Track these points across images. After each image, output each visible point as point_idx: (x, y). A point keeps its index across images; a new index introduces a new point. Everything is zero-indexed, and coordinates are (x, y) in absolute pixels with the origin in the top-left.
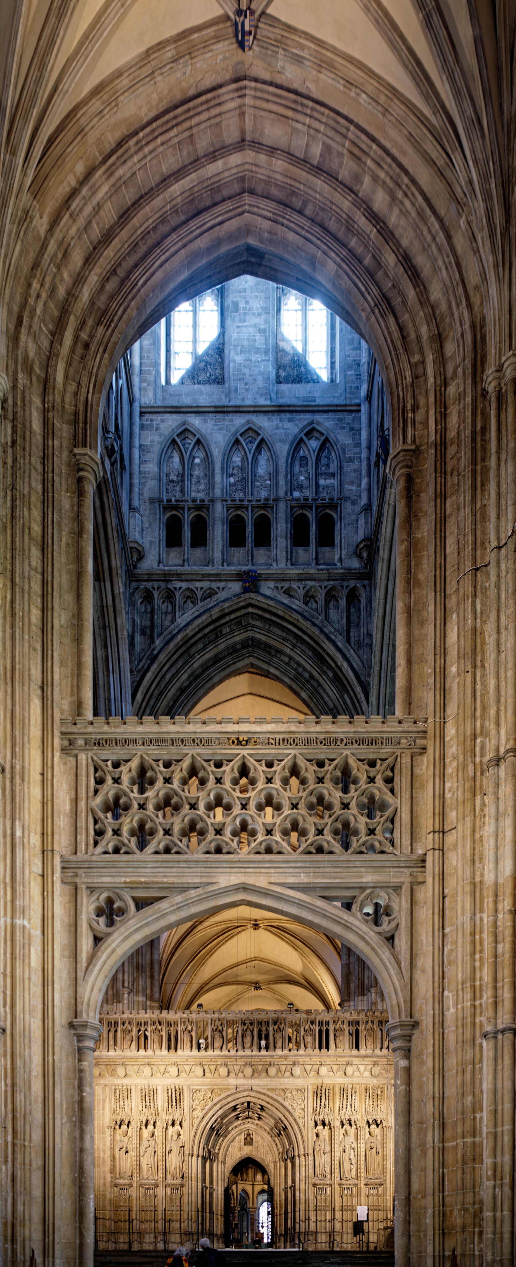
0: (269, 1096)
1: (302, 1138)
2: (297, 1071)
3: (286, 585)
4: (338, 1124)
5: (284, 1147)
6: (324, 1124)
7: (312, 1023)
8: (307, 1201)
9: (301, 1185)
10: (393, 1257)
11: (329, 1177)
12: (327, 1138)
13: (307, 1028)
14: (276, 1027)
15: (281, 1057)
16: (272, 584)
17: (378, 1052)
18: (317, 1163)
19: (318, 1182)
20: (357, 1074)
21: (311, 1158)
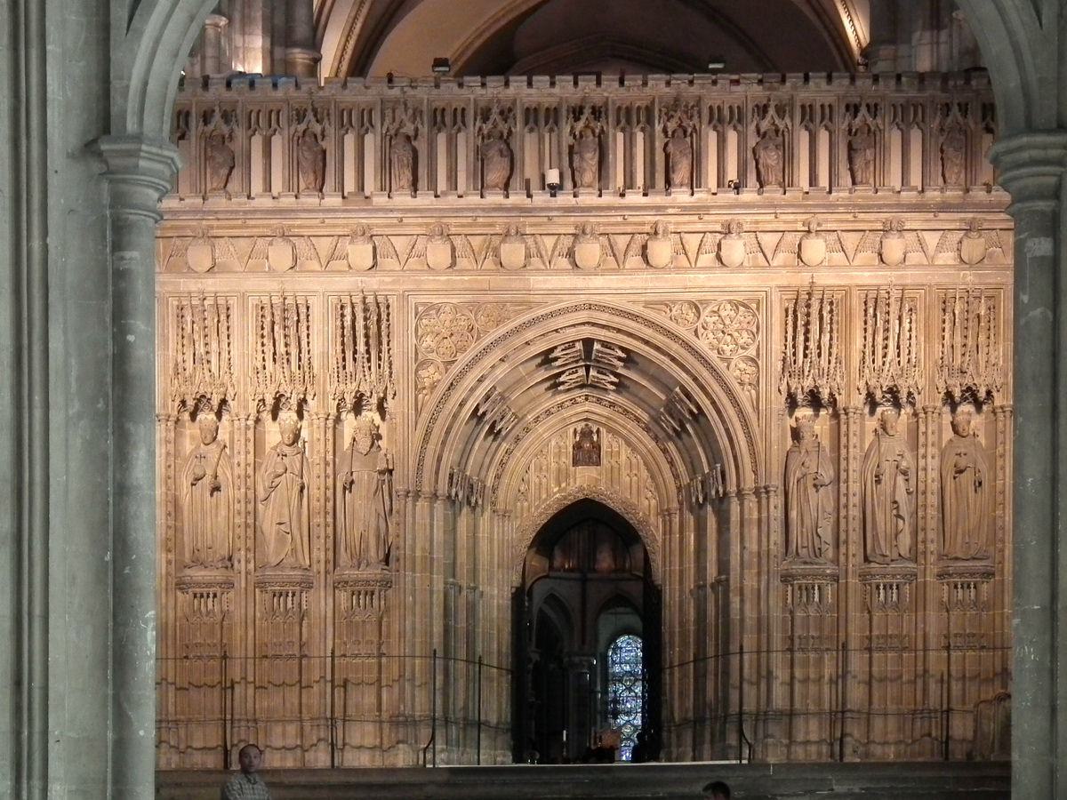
0: (650, 324)
2: (736, 249)
4: (858, 400)
5: (693, 468)
6: (815, 400)
7: (780, 111)
8: (762, 625)
10: (1007, 779)
11: (830, 554)
12: (826, 442)
13: (765, 125)
14: (672, 126)
15: (685, 210)
17: (979, 194)
18: (794, 514)
19: (798, 568)
20: (915, 257)
21: (776, 501)
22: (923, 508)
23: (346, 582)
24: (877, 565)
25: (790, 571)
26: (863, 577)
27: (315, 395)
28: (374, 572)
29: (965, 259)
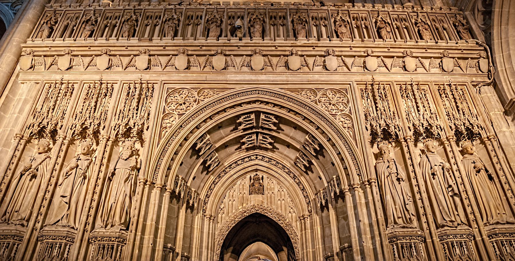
0: (290, 99)
1: (354, 158)
19: (399, 231)
22: (465, 193)
23: (96, 238)
24: (449, 228)
25: (395, 233)
27: (104, 127)
29: (446, 70)
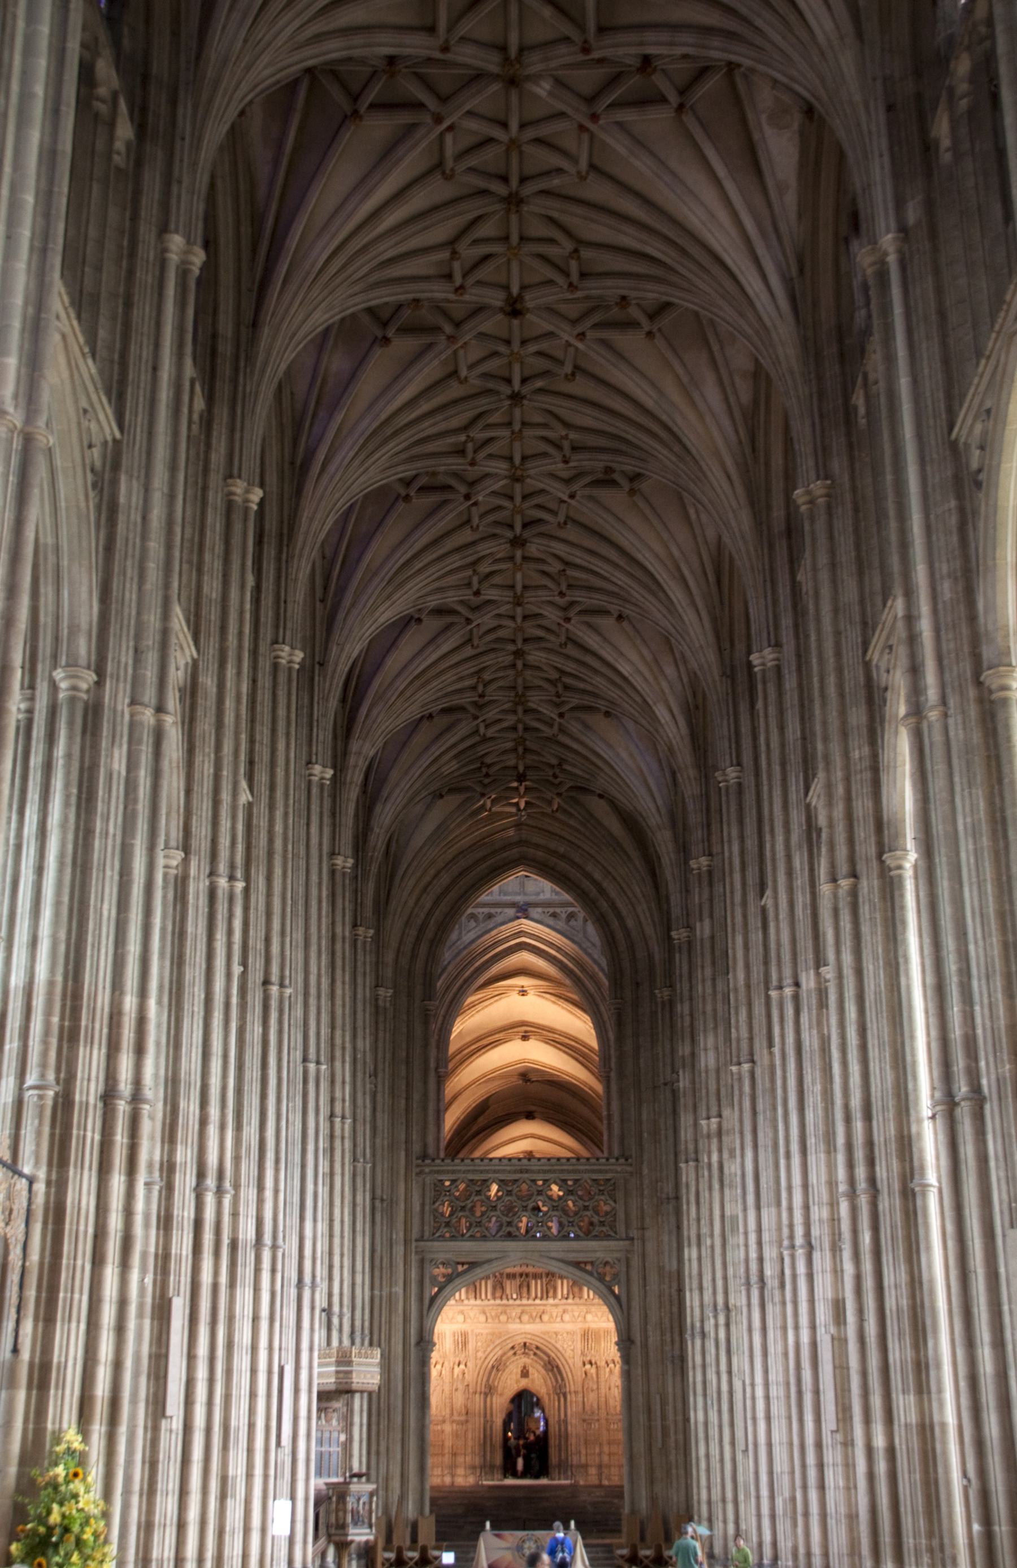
2: (567, 1317)
3: (551, 910)
4: (603, 1363)
6: (591, 1363)
9: (573, 1421)
16: (540, 910)
26: (607, 1420)
28: (463, 1418)
